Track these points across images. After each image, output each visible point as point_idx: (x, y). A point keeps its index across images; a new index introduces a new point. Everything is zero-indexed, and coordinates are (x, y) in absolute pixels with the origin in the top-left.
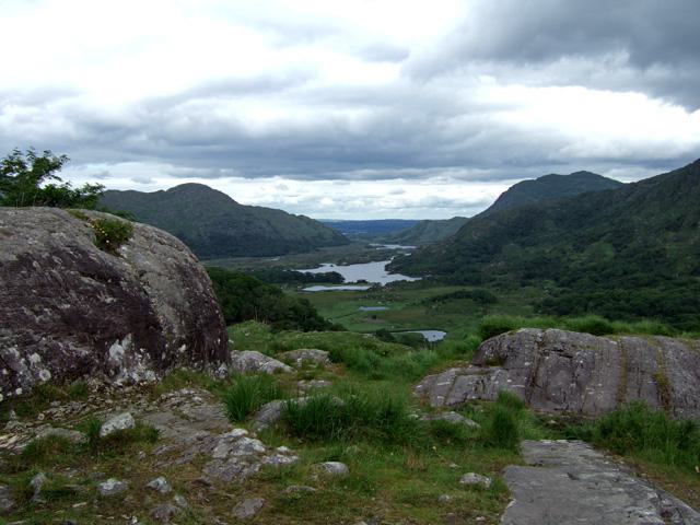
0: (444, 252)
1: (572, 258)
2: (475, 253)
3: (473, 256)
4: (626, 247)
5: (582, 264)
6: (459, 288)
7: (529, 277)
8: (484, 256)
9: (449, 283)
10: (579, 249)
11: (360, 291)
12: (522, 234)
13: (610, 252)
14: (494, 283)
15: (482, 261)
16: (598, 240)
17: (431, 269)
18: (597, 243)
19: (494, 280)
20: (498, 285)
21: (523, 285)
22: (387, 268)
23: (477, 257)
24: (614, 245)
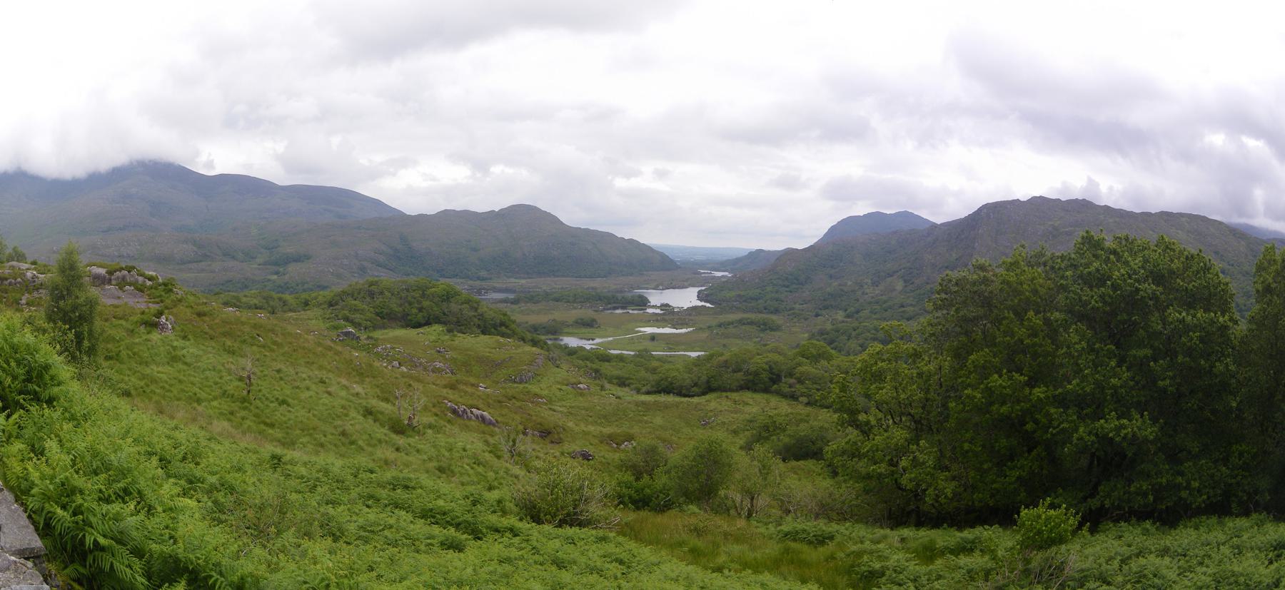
0: (757, 281)
1: (868, 291)
2: (786, 283)
3: (784, 286)
4: (913, 283)
5: (873, 297)
6: (752, 316)
7: (826, 308)
8: (794, 286)
9: (745, 311)
10: (876, 284)
11: (656, 314)
12: (832, 267)
13: (899, 286)
14: (790, 312)
15: (791, 292)
16: (892, 276)
17: (739, 296)
18: (891, 278)
19: (793, 309)
20: (794, 314)
21: (817, 315)
22: (699, 292)
23: (787, 287)
24: (905, 281)
